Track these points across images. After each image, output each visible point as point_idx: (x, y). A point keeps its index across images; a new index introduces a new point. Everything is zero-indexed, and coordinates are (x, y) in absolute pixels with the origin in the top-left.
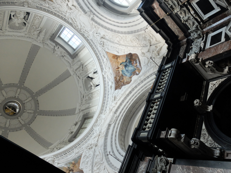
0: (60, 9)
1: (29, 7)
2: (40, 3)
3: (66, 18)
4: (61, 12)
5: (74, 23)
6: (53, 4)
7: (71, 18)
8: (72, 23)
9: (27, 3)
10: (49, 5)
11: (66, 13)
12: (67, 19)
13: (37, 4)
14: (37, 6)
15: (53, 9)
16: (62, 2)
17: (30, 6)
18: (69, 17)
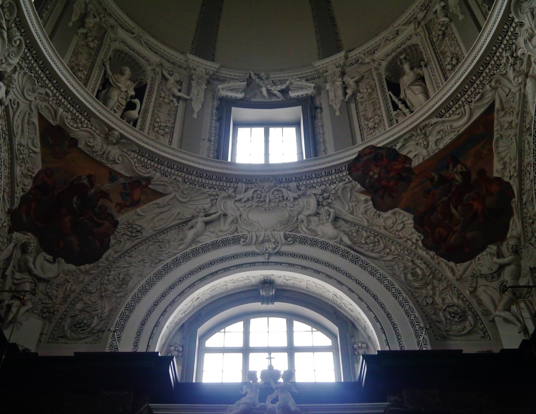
0: (29, 86)
1: (111, 129)
2: (75, 125)
3: (26, 51)
4: (31, 76)
5: (7, 21)
6: (43, 107)
7: (10, 41)
8: (13, 25)
9: (110, 139)
10: (56, 112)
11: (18, 68)
12: (24, 47)
13: (85, 126)
14: (86, 122)
15: (51, 94)
16: (15, 107)
17: (107, 129)
18: (15, 49)
